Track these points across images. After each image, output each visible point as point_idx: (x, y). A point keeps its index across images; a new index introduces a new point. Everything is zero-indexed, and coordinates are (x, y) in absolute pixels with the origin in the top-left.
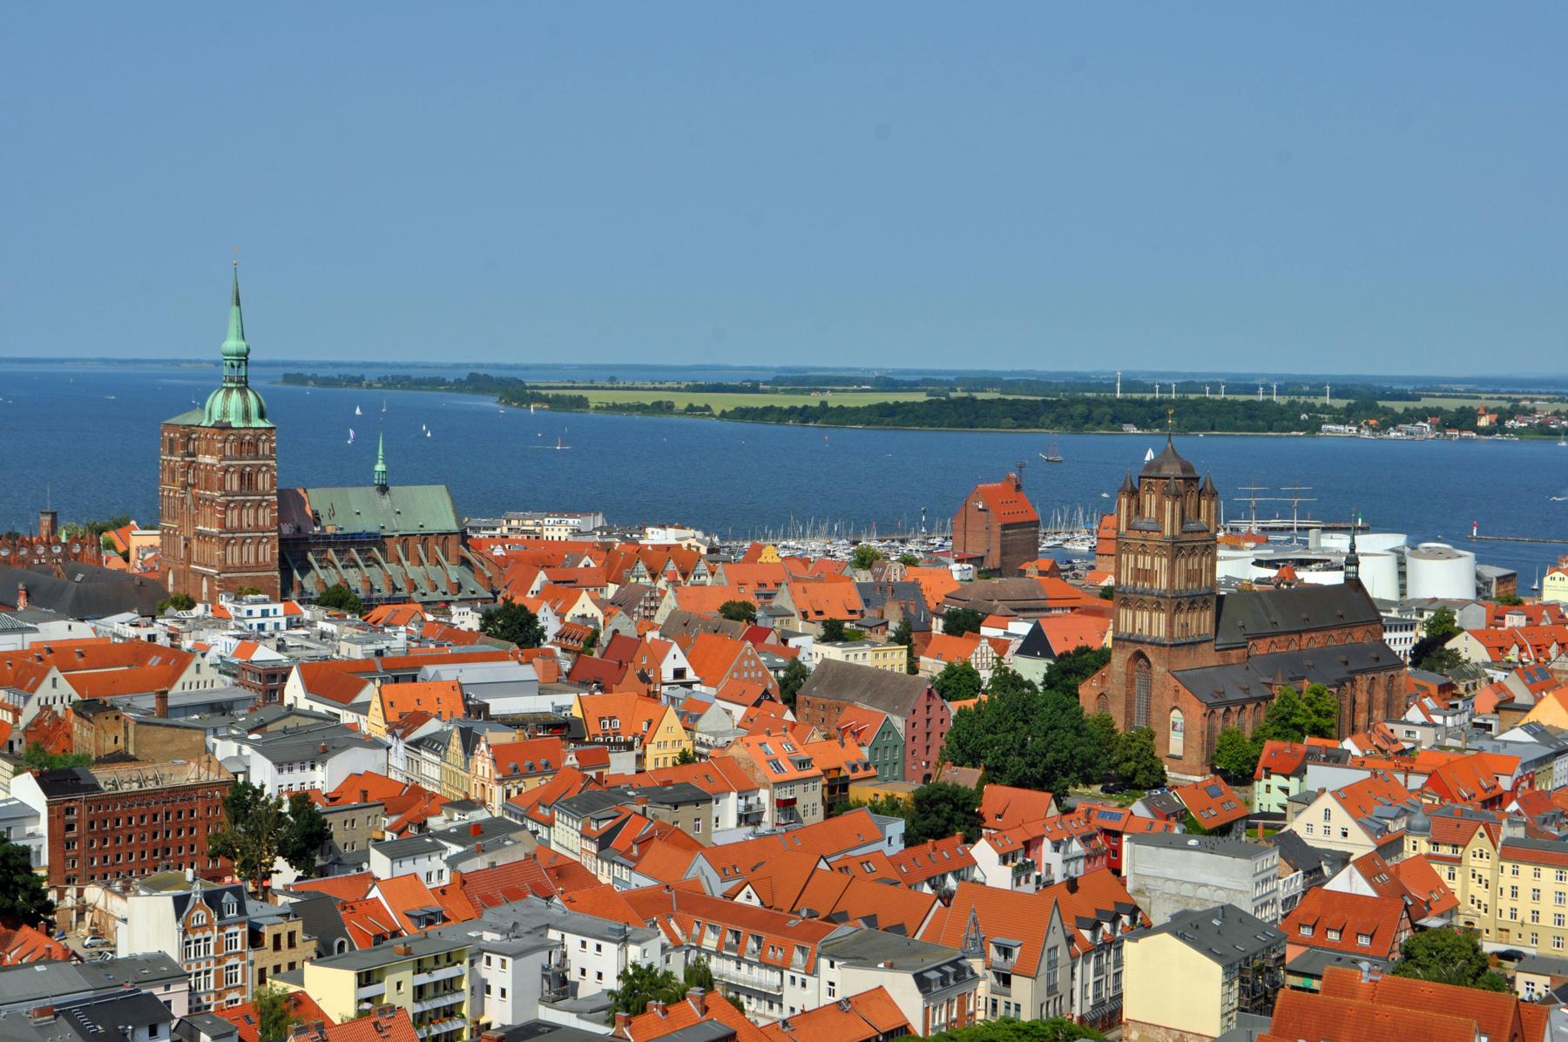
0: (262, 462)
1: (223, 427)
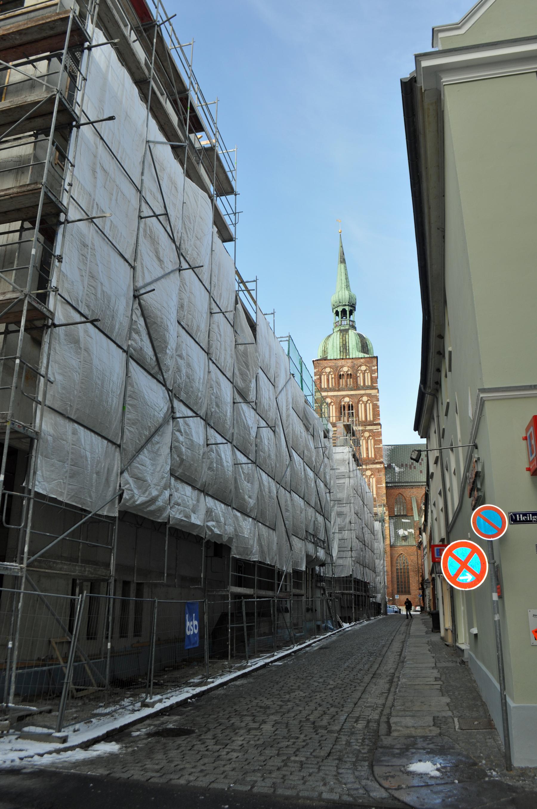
0: (362, 392)
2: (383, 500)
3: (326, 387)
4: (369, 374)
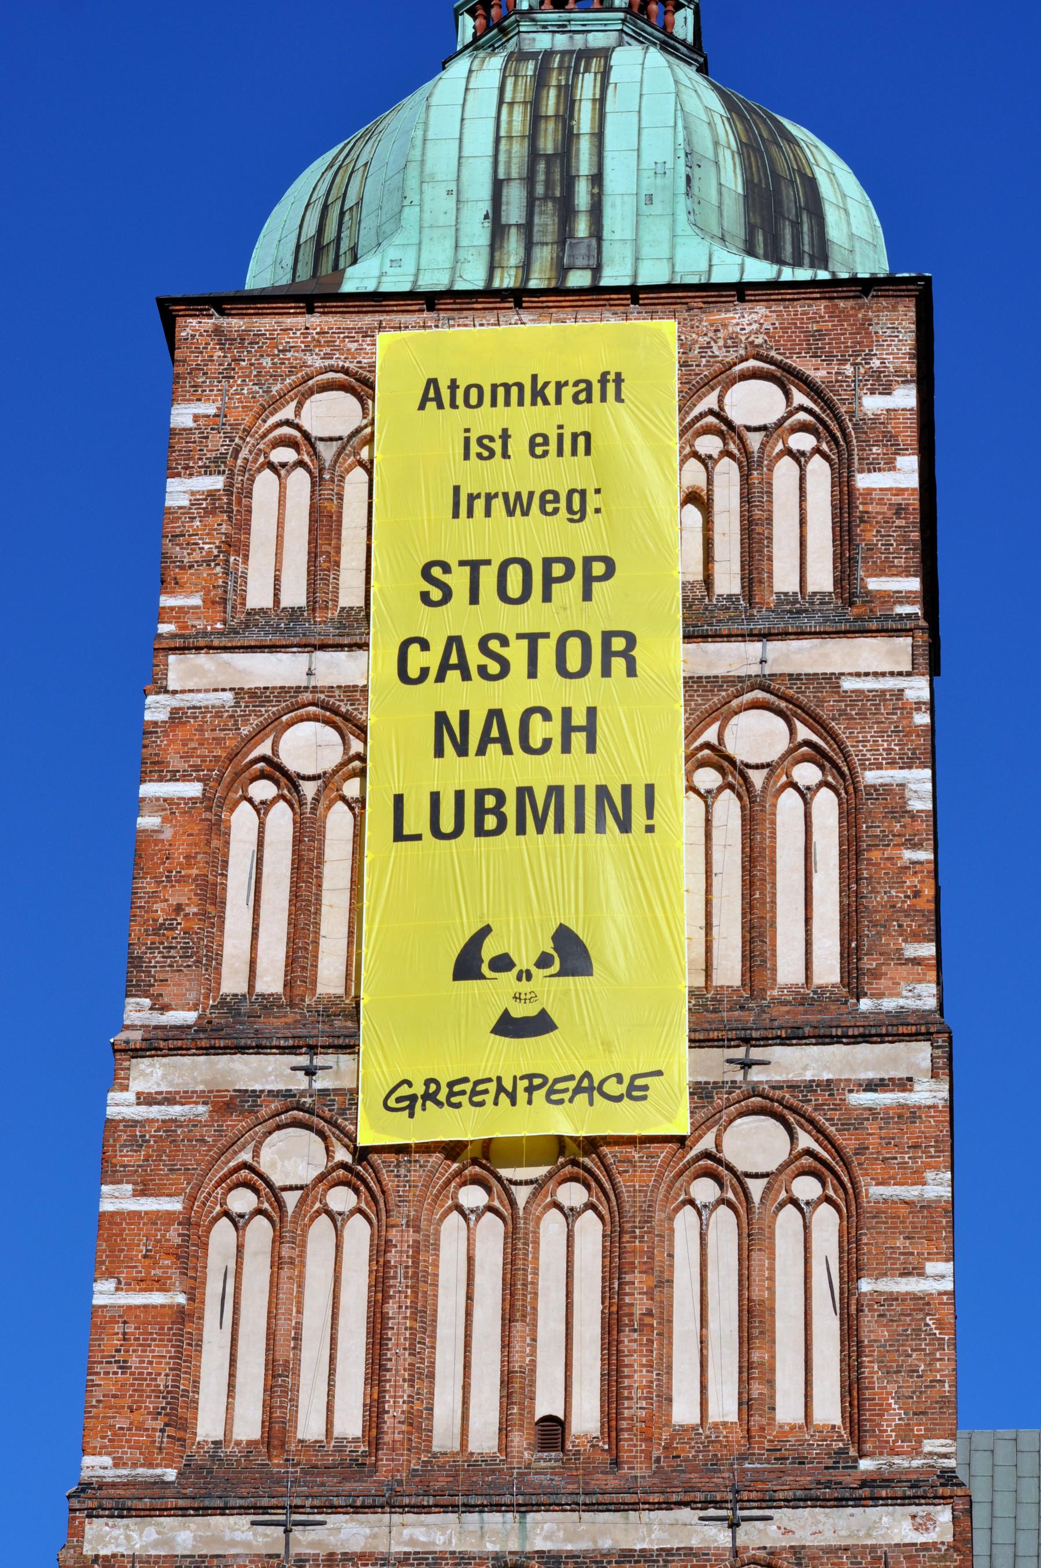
3: (295, 595)
4: (819, 471)
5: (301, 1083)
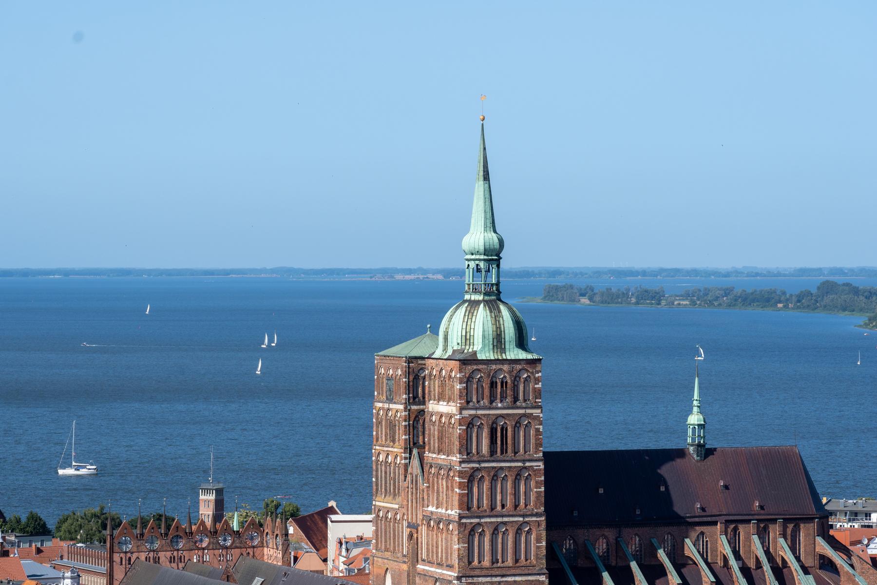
1: (468, 361)
2: (542, 564)
5: (478, 466)
